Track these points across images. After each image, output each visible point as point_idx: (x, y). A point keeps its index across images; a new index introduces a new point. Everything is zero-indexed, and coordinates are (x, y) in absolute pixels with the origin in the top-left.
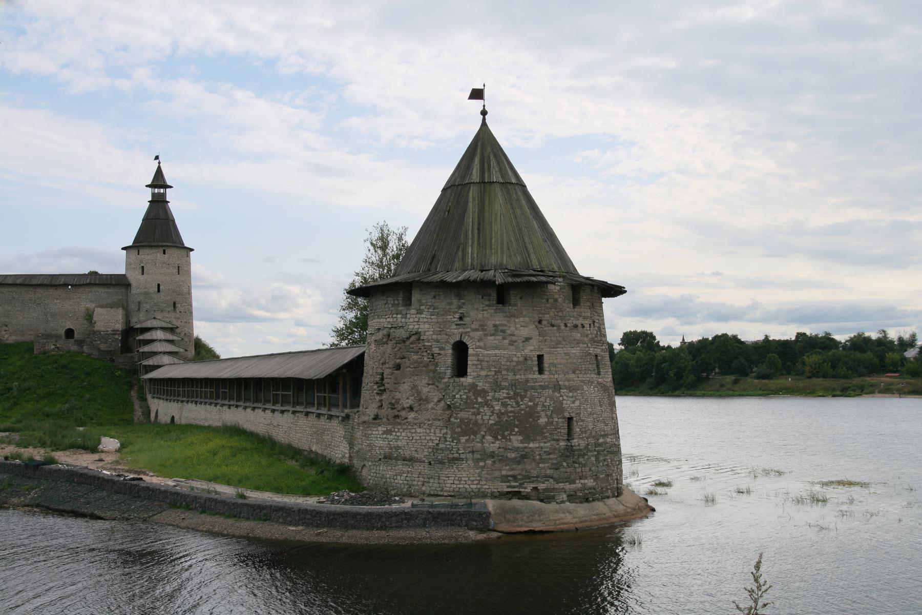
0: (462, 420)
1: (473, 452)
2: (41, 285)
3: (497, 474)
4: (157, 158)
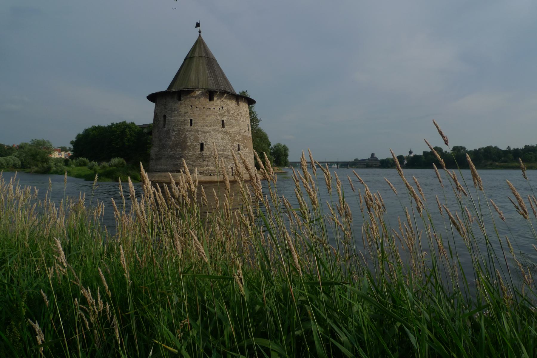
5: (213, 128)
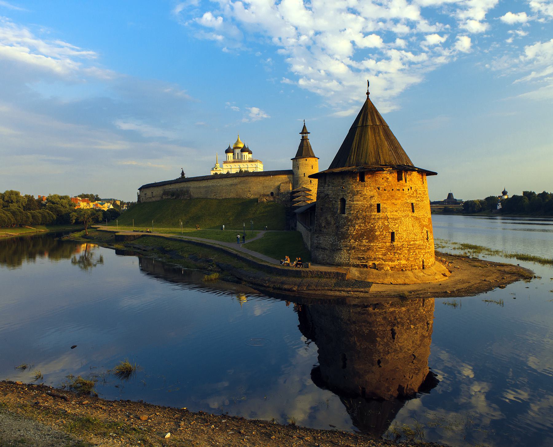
0: (342, 232)
1: (346, 246)
3: (356, 256)
5: (404, 214)
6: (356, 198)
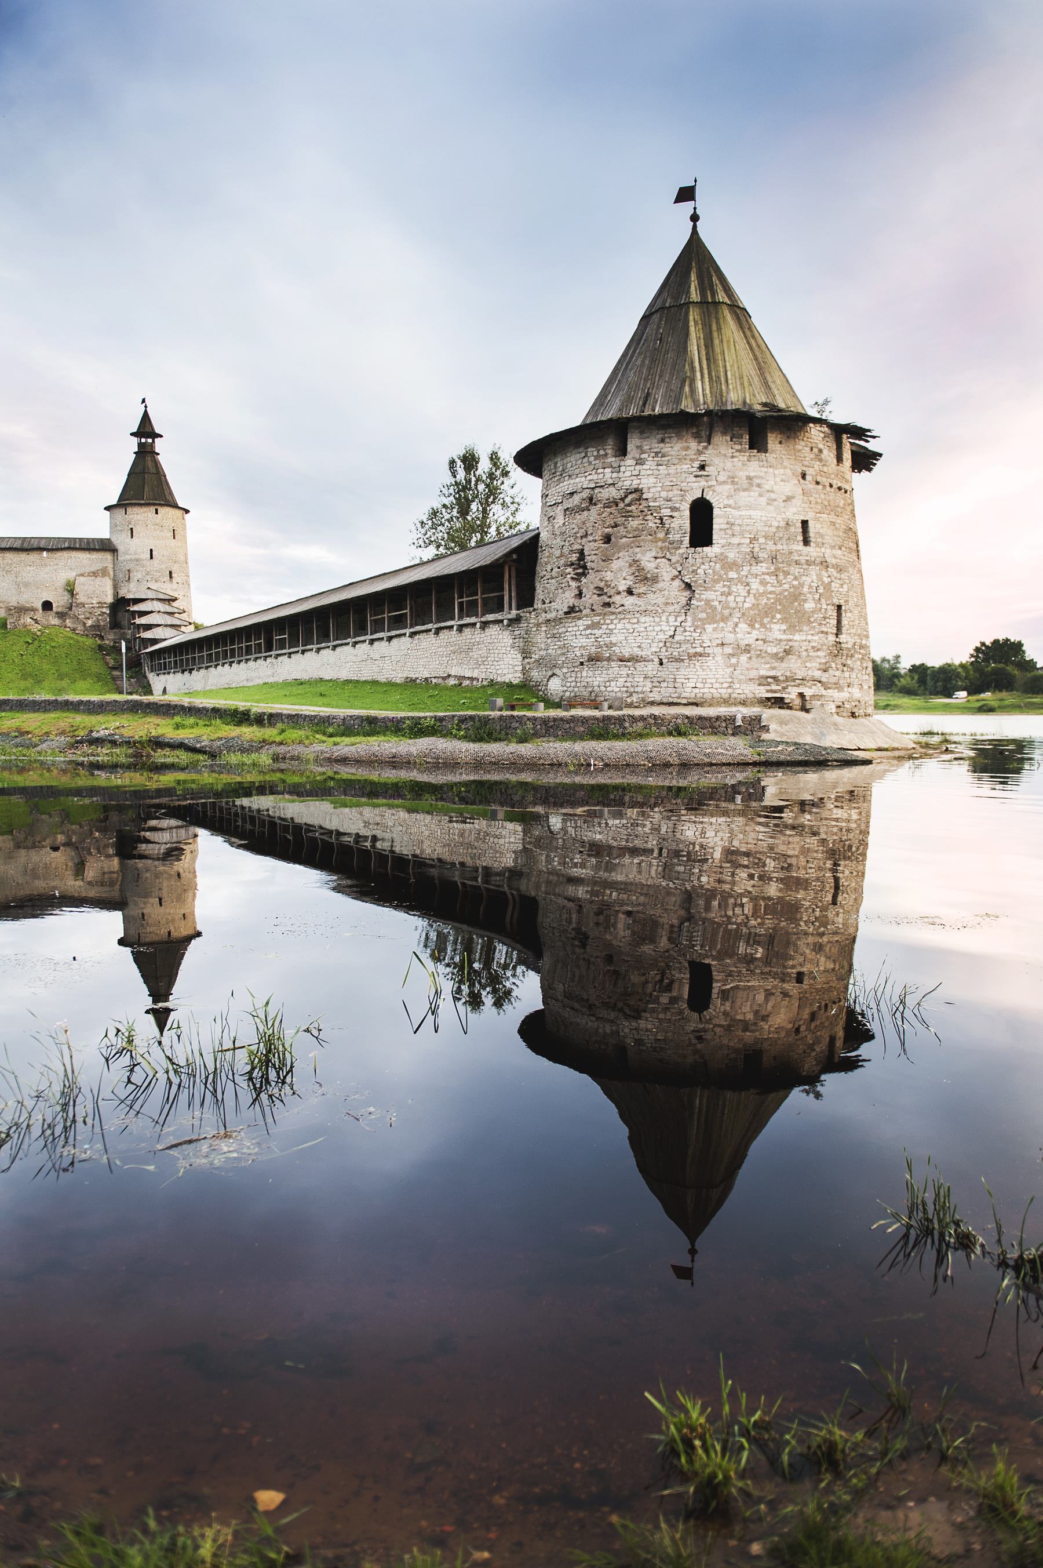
0: (708, 602)
2: (10, 549)
3: (753, 674)
4: (144, 401)
6: (744, 497)
